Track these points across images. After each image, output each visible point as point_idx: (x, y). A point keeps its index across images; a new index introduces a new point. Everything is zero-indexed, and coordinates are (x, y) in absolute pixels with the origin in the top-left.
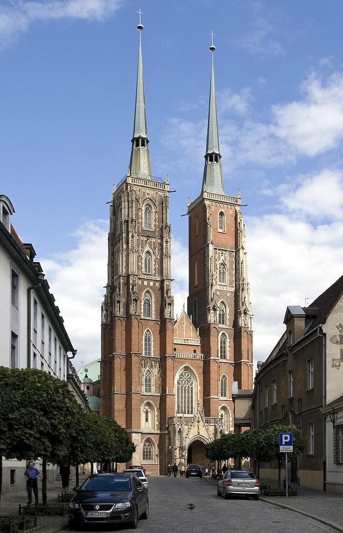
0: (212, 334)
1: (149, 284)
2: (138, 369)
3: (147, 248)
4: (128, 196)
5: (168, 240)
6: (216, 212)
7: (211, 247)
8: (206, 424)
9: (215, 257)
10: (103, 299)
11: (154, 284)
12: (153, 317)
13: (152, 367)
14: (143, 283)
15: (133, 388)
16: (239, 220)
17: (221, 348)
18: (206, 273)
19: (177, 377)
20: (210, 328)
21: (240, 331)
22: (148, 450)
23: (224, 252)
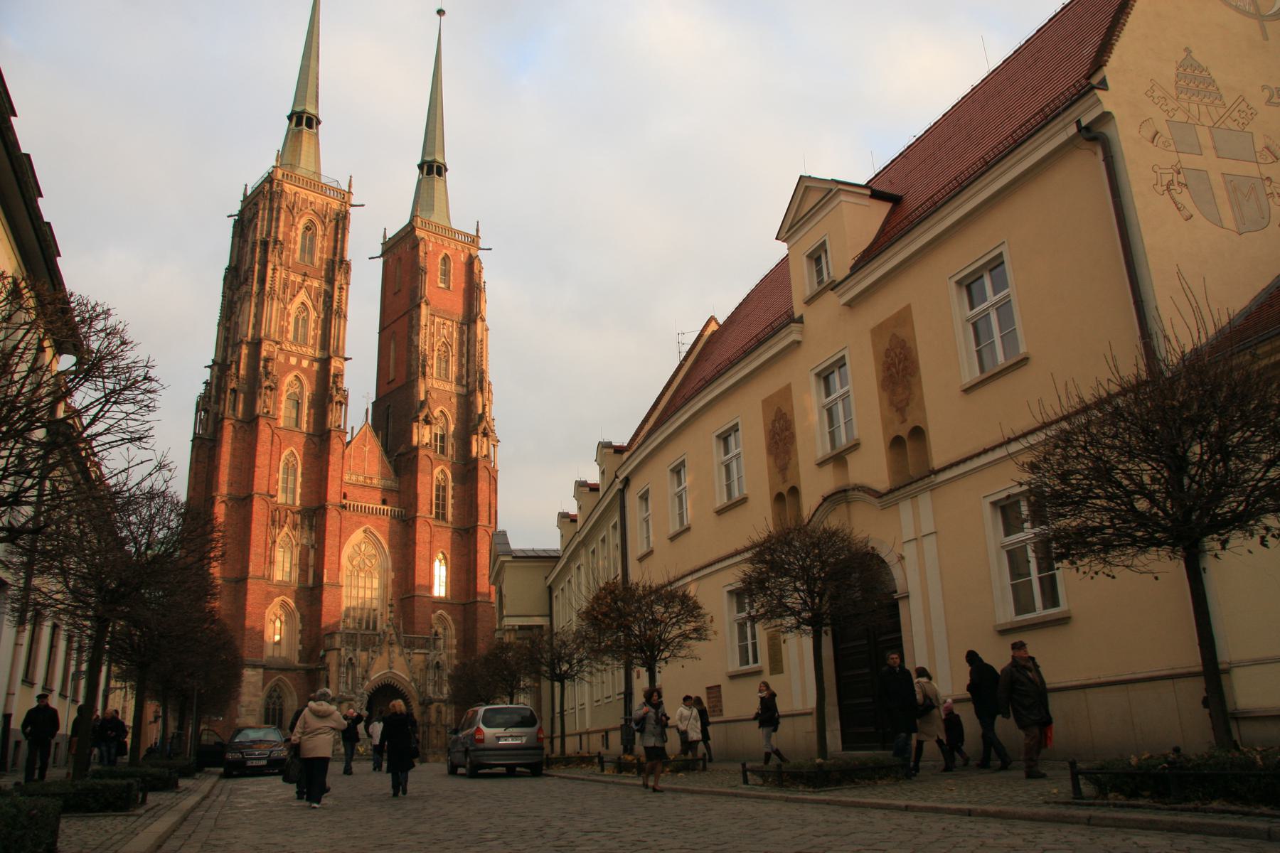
0: (421, 466)
1: (299, 362)
2: (263, 529)
3: (302, 296)
4: (271, 200)
5: (345, 287)
6: (436, 254)
7: (424, 310)
8: (406, 650)
9: (430, 330)
10: (201, 389)
11: (311, 365)
12: (304, 427)
13: (295, 527)
14: (288, 359)
15: (251, 569)
16: (476, 271)
17: (438, 497)
18: (414, 355)
19: (347, 550)
20: (416, 457)
21: (476, 469)
22: (277, 708)
23: (449, 323)
